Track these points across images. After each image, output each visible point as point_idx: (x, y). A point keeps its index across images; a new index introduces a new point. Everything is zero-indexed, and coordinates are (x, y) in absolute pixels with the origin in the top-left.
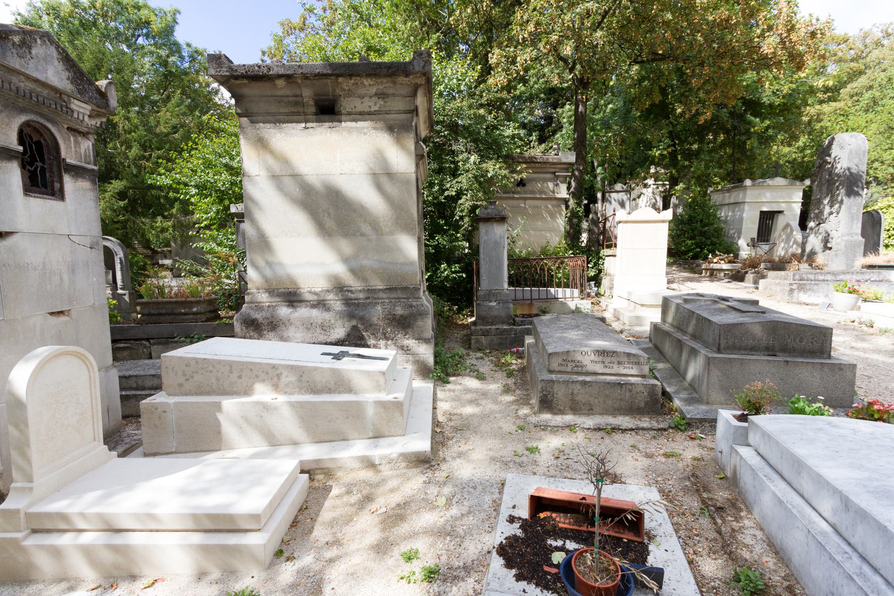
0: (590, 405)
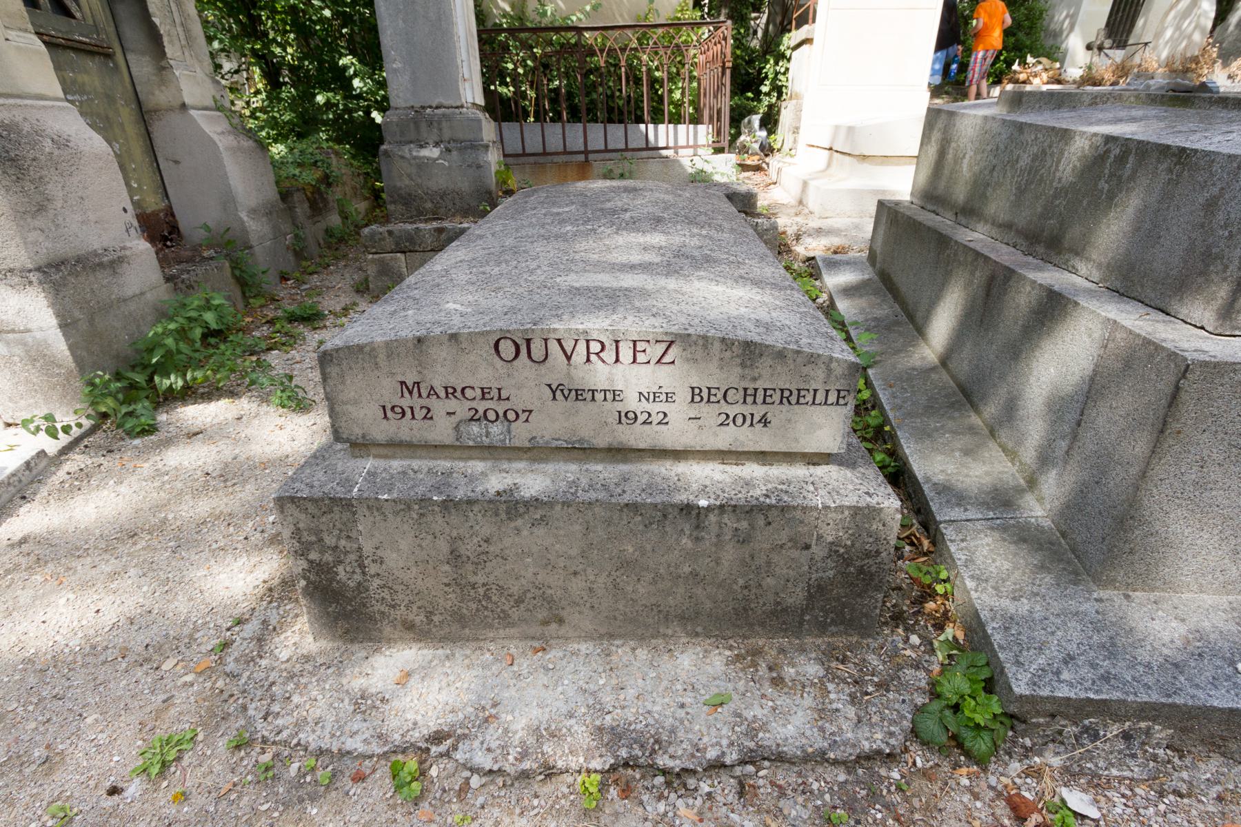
0: (550, 601)
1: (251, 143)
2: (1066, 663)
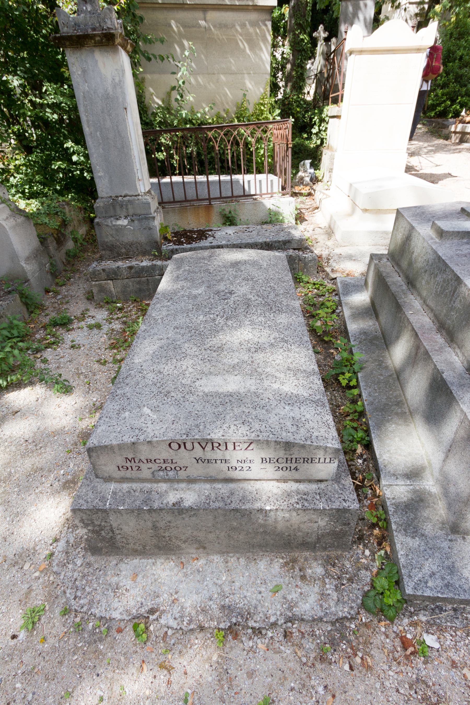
1: (22, 218)
2: (431, 577)
